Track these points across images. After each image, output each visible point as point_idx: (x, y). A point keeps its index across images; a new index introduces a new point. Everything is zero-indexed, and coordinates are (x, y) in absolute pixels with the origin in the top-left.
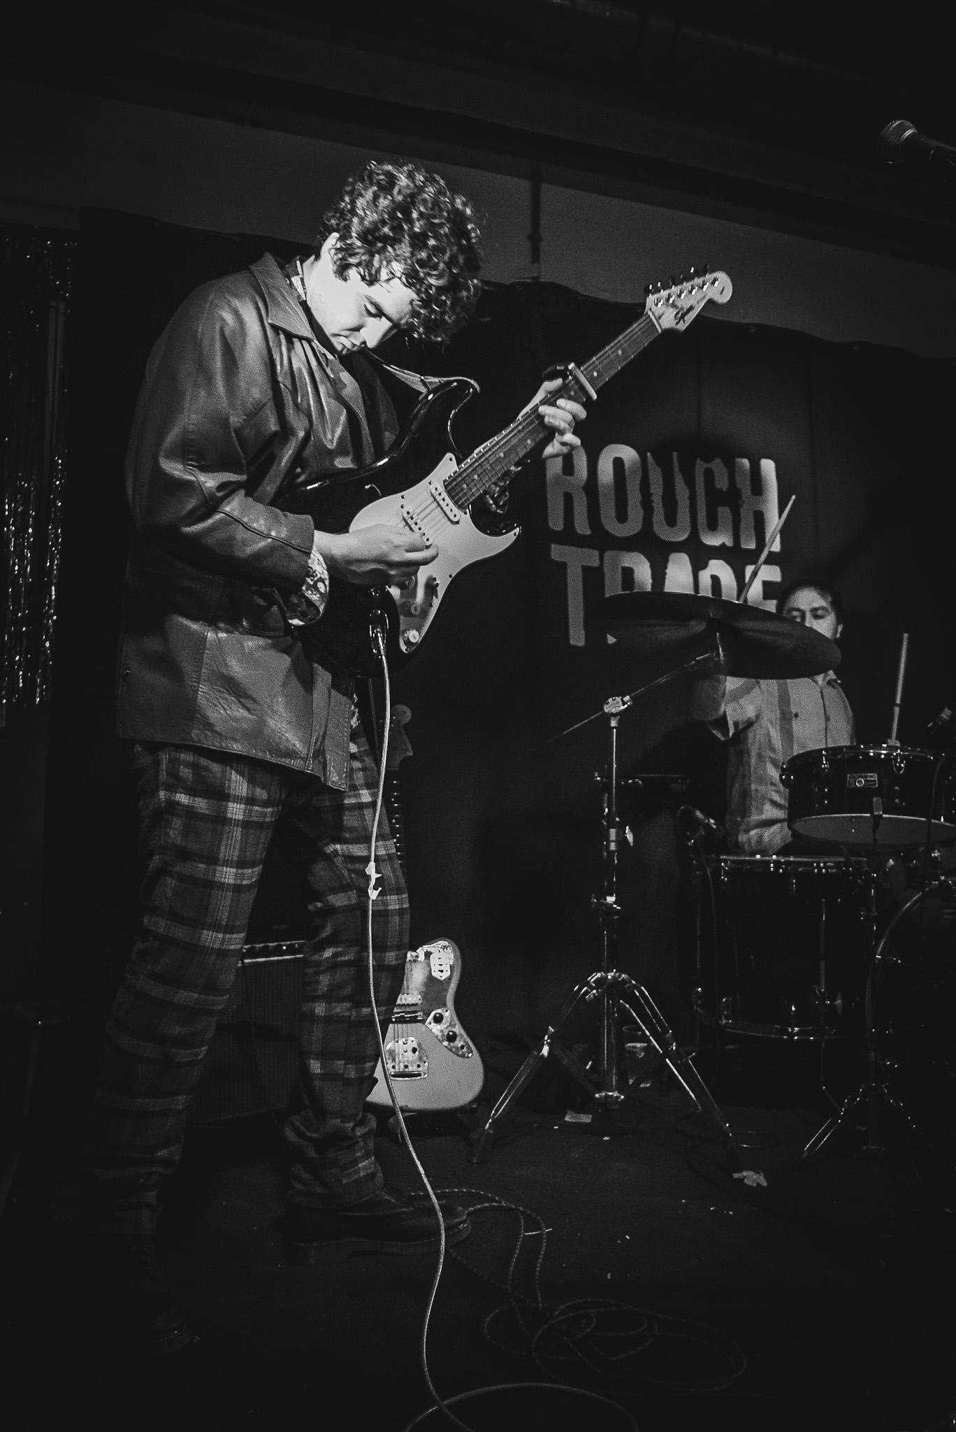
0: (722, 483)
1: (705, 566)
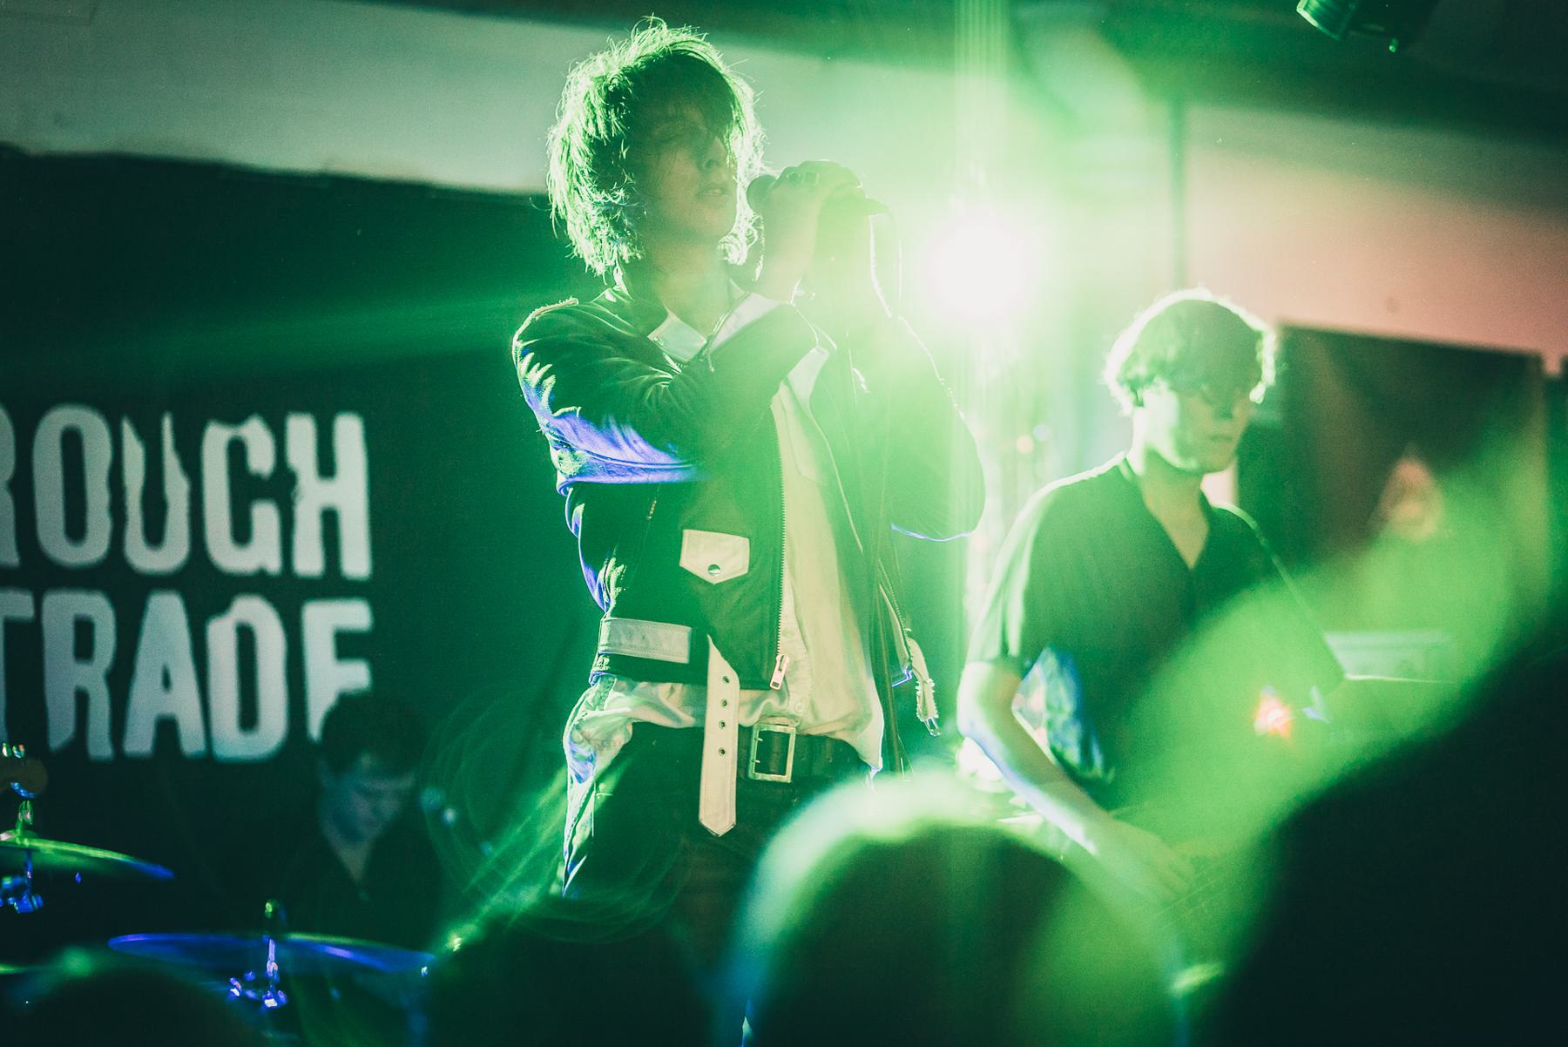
0: (261, 460)
1: (222, 607)
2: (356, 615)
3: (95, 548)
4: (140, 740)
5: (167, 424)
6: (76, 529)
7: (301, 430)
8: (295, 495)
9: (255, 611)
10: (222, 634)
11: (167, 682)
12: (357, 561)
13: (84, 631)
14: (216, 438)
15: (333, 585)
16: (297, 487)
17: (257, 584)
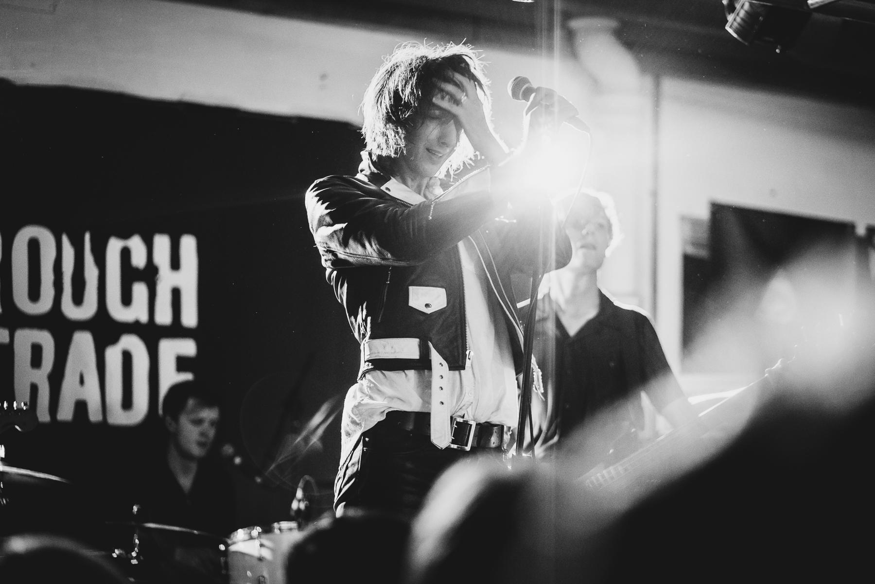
0: (139, 260)
1: (115, 340)
2: (188, 347)
3: (44, 305)
4: (66, 413)
5: (87, 237)
6: (34, 294)
7: (162, 243)
8: (157, 279)
9: (132, 343)
10: (113, 355)
11: (82, 382)
12: (190, 318)
13: (37, 351)
14: (114, 246)
15: (176, 330)
16: (158, 276)
17: (134, 328)
